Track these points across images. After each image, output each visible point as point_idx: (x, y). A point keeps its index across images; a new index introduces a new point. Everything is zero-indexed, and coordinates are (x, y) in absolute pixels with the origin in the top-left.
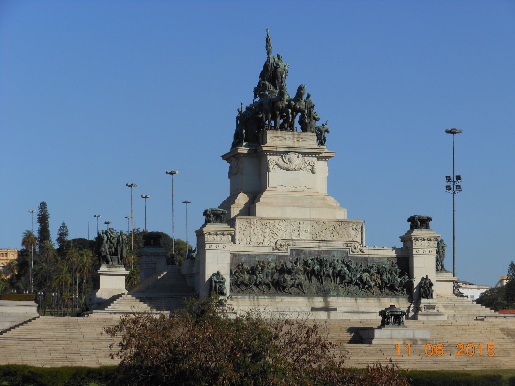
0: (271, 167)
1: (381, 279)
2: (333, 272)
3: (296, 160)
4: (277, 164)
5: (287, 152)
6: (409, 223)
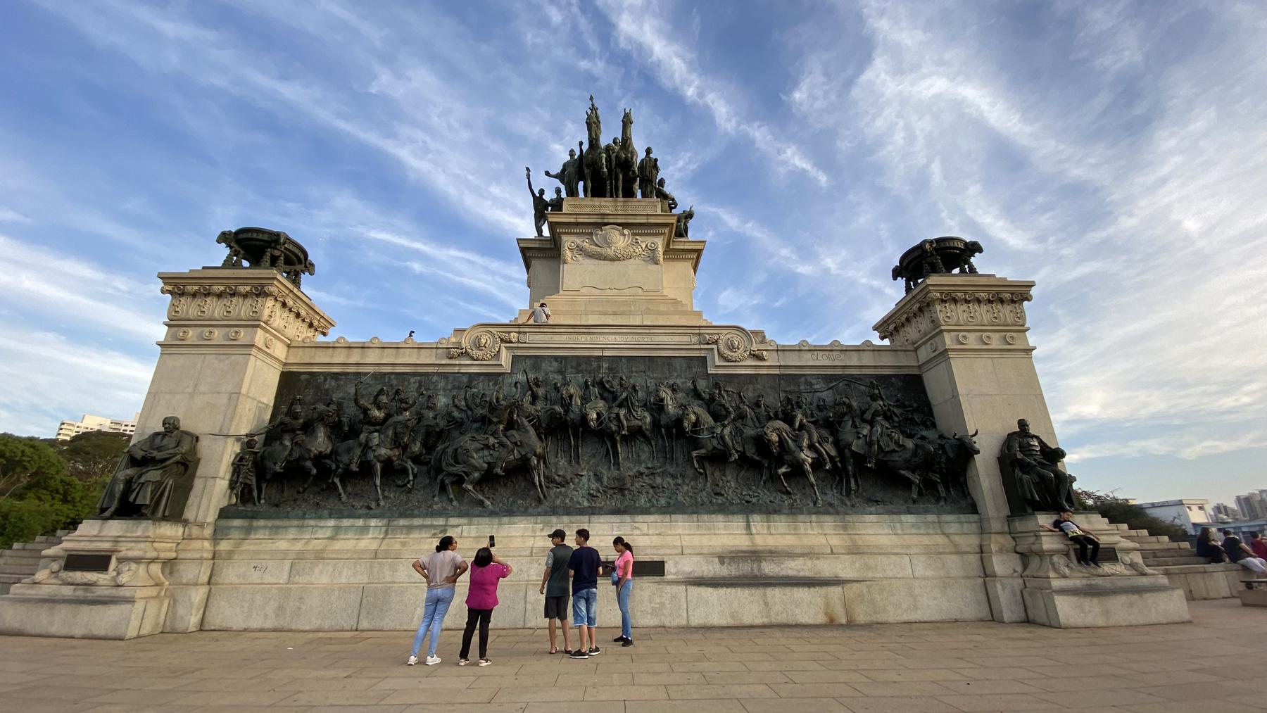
0: (568, 254)
1: (836, 443)
2: (656, 424)
3: (620, 241)
4: (581, 250)
5: (600, 225)
6: (901, 282)
